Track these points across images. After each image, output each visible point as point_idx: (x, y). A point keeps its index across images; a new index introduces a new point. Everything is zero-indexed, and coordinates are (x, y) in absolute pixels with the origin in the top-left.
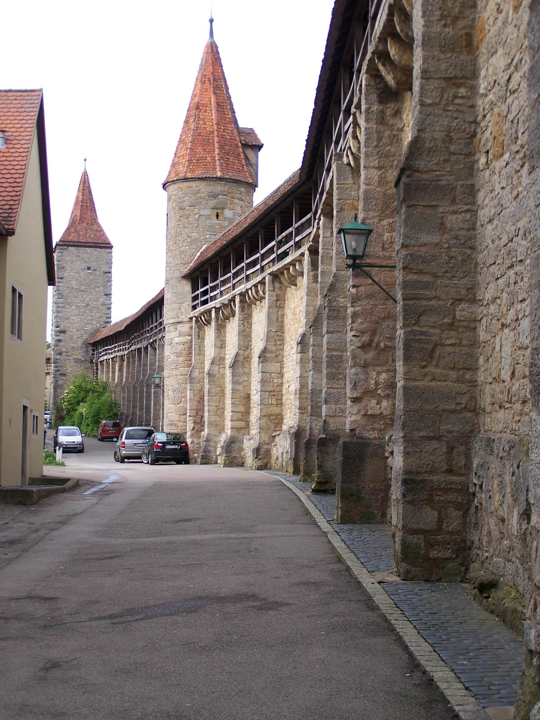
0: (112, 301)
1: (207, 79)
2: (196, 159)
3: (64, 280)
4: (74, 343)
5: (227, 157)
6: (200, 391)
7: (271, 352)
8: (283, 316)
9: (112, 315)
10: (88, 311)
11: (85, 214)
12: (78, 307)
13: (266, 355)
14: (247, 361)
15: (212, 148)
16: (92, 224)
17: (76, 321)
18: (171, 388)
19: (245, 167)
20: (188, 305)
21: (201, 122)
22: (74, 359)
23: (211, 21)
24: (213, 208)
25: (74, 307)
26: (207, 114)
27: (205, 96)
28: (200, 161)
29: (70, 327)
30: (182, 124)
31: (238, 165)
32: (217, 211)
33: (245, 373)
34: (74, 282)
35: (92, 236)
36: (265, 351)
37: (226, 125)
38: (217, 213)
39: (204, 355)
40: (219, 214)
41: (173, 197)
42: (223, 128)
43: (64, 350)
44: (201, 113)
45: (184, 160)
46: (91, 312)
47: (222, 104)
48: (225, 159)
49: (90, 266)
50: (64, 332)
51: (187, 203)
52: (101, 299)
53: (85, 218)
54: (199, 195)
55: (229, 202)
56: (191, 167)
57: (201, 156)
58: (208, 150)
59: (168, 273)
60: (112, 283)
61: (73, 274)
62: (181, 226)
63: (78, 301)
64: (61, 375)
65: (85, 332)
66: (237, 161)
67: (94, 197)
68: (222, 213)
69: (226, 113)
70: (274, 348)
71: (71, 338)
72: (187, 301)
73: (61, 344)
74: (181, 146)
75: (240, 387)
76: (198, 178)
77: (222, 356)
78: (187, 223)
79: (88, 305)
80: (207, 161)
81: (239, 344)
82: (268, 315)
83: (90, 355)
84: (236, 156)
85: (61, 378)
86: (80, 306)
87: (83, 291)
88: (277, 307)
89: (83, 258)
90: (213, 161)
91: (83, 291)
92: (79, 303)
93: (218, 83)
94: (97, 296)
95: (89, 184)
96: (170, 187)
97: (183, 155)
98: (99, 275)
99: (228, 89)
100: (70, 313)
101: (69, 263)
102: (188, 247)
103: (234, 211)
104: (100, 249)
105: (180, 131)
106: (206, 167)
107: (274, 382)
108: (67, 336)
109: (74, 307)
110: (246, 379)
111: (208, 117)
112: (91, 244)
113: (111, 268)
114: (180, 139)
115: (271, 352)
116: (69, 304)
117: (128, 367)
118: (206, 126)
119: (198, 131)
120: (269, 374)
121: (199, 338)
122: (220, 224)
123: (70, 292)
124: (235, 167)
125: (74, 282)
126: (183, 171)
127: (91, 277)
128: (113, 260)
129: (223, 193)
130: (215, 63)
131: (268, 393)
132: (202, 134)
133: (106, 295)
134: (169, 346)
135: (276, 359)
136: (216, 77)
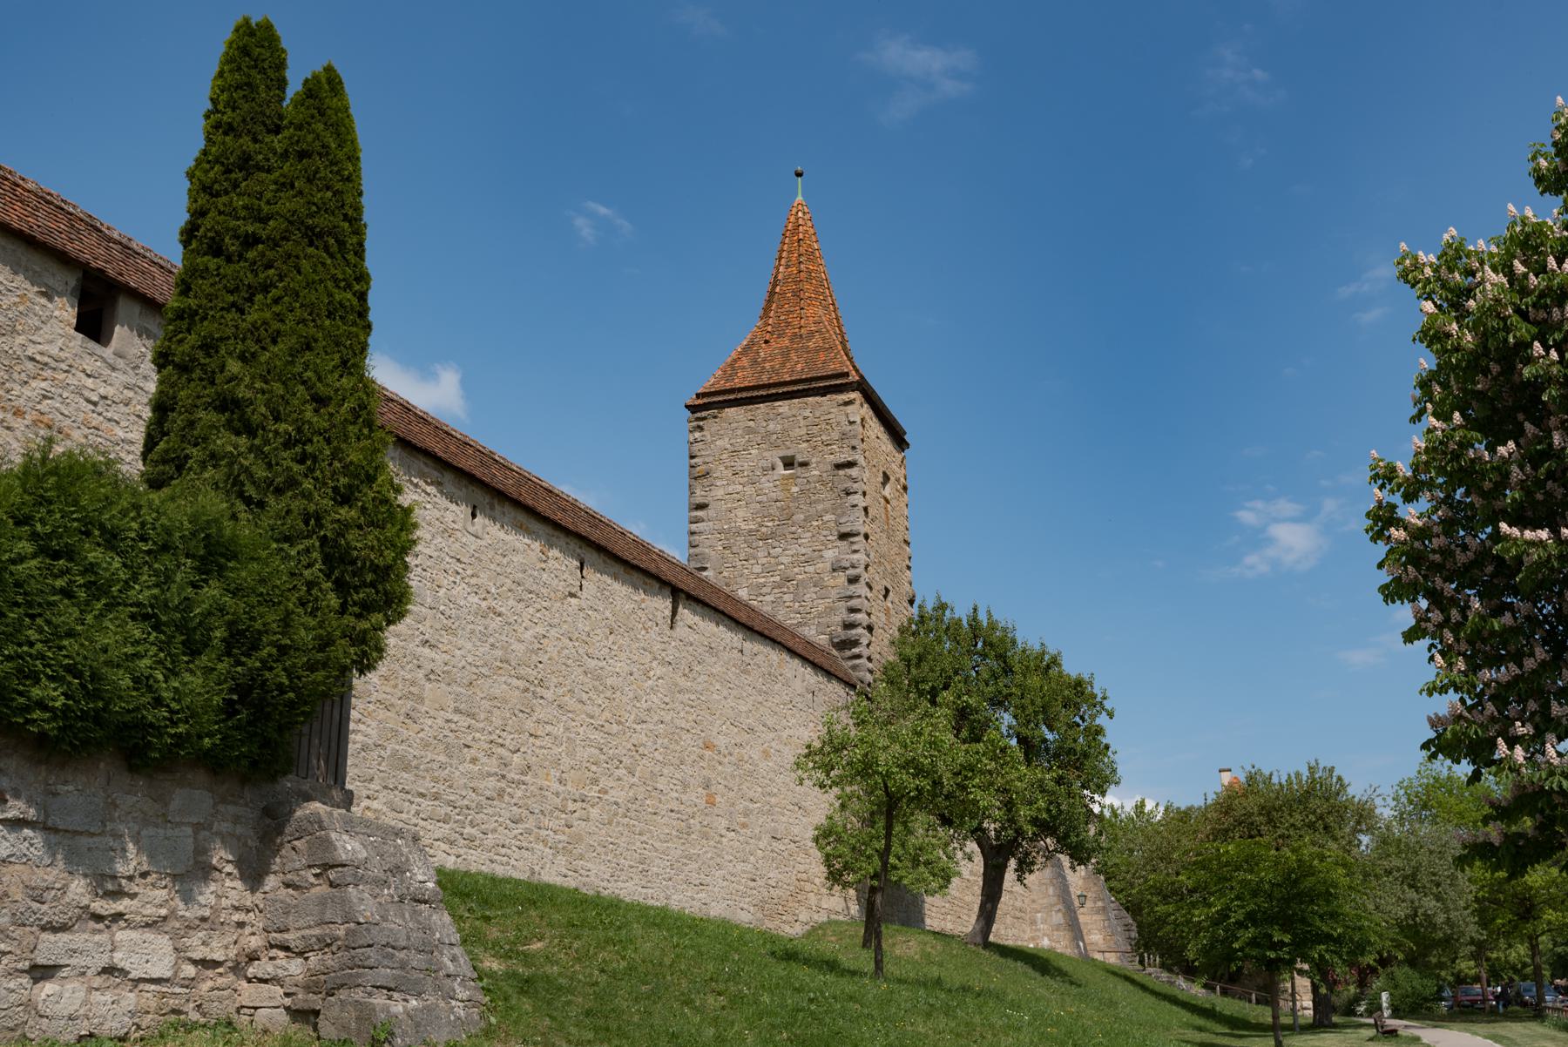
3: (710, 512)
10: (786, 597)
34: (741, 513)
49: (789, 453)
52: (830, 554)
53: (788, 324)
87: (773, 535)
91: (773, 535)
98: (820, 480)
101: (725, 456)
104: (818, 399)
127: (795, 489)
133: (843, 536)
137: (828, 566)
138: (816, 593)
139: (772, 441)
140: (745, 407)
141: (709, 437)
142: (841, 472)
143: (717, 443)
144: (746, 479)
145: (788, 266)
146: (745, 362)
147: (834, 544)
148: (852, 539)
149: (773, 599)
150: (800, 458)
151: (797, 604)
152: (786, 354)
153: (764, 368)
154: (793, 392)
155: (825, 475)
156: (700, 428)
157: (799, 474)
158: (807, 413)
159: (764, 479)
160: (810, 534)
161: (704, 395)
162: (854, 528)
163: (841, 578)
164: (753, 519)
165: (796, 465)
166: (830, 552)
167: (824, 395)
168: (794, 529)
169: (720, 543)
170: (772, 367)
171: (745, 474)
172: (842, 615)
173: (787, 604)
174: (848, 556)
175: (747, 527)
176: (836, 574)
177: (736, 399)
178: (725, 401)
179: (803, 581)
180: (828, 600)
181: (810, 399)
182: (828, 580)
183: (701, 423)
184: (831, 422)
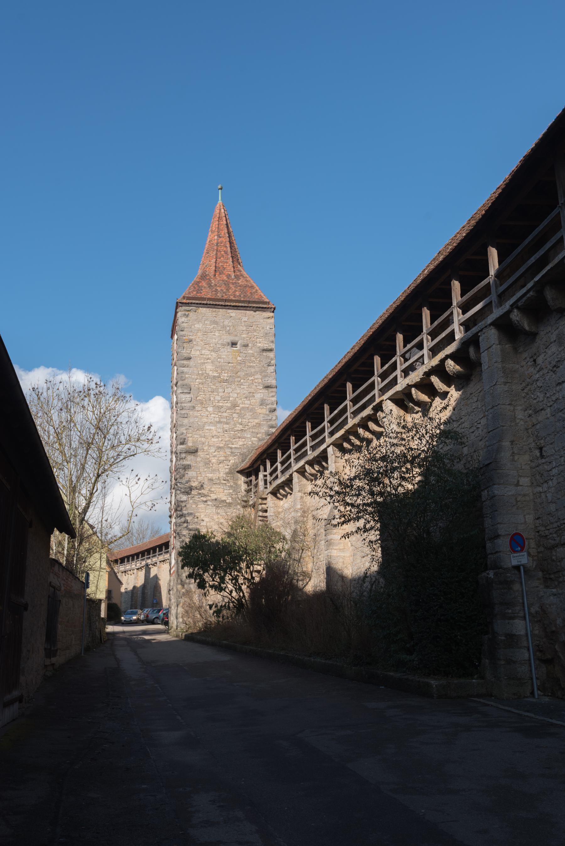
3: (191, 363)
4: (213, 471)
10: (235, 415)
25: (210, 409)
34: (209, 367)
35: (237, 293)
43: (194, 484)
50: (194, 452)
52: (258, 396)
61: (208, 352)
65: (232, 453)
71: (207, 463)
79: (234, 406)
86: (222, 407)
87: (226, 381)
89: (224, 327)
91: (226, 381)
94: (252, 390)
100: (205, 420)
101: (199, 334)
108: (199, 459)
109: (210, 409)
116: (202, 403)
125: (209, 367)
127: (240, 359)
138: (251, 415)
140: (211, 309)
142: (264, 354)
143: (196, 326)
144: (212, 348)
147: (260, 391)
148: (270, 390)
154: (239, 306)
155: (256, 354)
156: (187, 316)
157: (242, 351)
158: (245, 319)
160: (248, 383)
161: (189, 298)
163: (264, 411)
167: (255, 311)
168: (239, 379)
169: (197, 380)
170: (222, 290)
171: (212, 345)
174: (268, 398)
175: (213, 374)
176: (261, 407)
177: (206, 304)
178: (200, 304)
179: (243, 408)
180: (257, 420)
181: (248, 312)
183: (187, 313)
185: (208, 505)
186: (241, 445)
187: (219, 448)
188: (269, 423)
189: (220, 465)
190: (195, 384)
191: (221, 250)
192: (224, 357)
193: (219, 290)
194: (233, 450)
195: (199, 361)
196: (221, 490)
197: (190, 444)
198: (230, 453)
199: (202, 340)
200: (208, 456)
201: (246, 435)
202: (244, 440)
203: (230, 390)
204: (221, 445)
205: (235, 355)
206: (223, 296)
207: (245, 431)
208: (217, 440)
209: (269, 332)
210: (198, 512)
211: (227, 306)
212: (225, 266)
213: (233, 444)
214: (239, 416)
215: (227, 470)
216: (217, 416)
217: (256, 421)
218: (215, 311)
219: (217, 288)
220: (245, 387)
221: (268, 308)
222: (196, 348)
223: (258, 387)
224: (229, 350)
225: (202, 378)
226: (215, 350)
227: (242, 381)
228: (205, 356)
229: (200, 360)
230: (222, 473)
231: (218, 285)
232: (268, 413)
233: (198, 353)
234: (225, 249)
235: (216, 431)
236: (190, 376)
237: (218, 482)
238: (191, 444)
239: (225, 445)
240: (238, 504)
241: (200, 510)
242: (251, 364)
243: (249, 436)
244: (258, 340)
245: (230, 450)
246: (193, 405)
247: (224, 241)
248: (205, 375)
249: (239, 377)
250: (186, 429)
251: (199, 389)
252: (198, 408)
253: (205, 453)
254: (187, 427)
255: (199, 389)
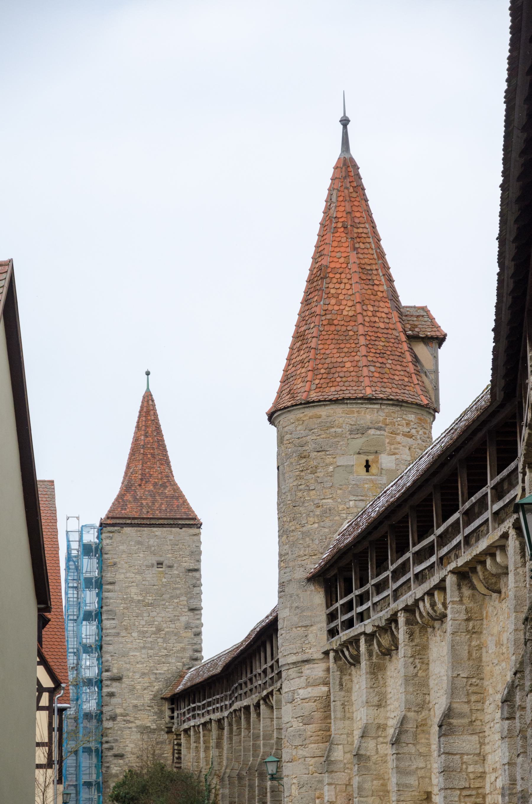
0: (204, 620)
1: (340, 225)
2: (326, 366)
3: (116, 587)
5: (380, 360)
6: (346, 785)
7: (461, 715)
8: (479, 648)
9: (203, 645)
11: (150, 468)
12: (143, 634)
13: (451, 721)
14: (423, 731)
15: (353, 345)
16: (164, 486)
17: (139, 659)
18: (295, 781)
19: (413, 375)
20: (321, 629)
21: (333, 301)
22: (137, 727)
23: (345, 122)
24: (359, 453)
25: (135, 634)
26: (342, 286)
27: (338, 255)
28: (333, 371)
29: (128, 670)
30: (298, 307)
31: (402, 373)
32: (366, 458)
33: (420, 754)
34: (134, 590)
35: (163, 507)
36: (448, 714)
37: (377, 303)
38: (367, 461)
39: (351, 719)
40: (370, 463)
41: (288, 437)
42: (371, 308)
43: (119, 711)
44: (331, 286)
45: (304, 370)
46: (165, 641)
47: (368, 267)
48: (378, 365)
49: (161, 559)
50: (118, 679)
51: (311, 446)
52: (183, 619)
53: (151, 476)
54: (333, 430)
55: (387, 441)
56: (317, 381)
57: (334, 360)
58: (346, 350)
59: (282, 572)
60: (202, 588)
62: (303, 486)
63: (143, 623)
64: (116, 756)
65: (156, 678)
66: (399, 368)
67: (165, 438)
68: (376, 461)
69: (376, 282)
70: (466, 708)
71: (132, 689)
72: (318, 623)
73: (114, 701)
74: (298, 344)
75: (412, 781)
76: (330, 400)
77: (382, 721)
78: (313, 481)
80: (344, 369)
81: (407, 701)
82: (453, 646)
83: (167, 719)
84: (396, 358)
85: (115, 761)
86: (147, 632)
87: (151, 605)
88: (468, 631)
89: (149, 547)
90: (356, 369)
91: (151, 605)
92: (143, 627)
93: (360, 230)
94: (176, 613)
95: (156, 415)
96: (281, 418)
97: (302, 362)
98: (178, 576)
99: (379, 240)
100: (129, 646)
101: (124, 556)
102: (316, 525)
103: (397, 456)
105: (295, 318)
106: (344, 379)
107: (469, 770)
108: (124, 686)
109: (135, 634)
110: (422, 765)
111: (344, 292)
112: (161, 522)
113: (199, 561)
114: (297, 332)
115: (461, 715)
116: (126, 629)
117: (231, 739)
118: (342, 307)
119: (328, 317)
120: (458, 757)
121: (341, 689)
122: (372, 481)
123: (127, 608)
124: (396, 378)
126: (303, 390)
128: (202, 548)
129: (377, 425)
130: (354, 195)
131: (458, 792)
132: (336, 322)
133: (192, 610)
134: (289, 705)
135: (471, 727)
136: (357, 221)
137: (183, 624)
139: (152, 551)
140: (136, 528)
141: (115, 543)
142: (190, 574)
143: (120, 547)
144: (137, 571)
145: (146, 436)
146: (129, 497)
147: (186, 614)
149: (151, 640)
150: (166, 562)
151: (165, 645)
152: (153, 496)
153: (142, 503)
155: (181, 574)
156: (111, 538)
157: (167, 572)
158: (171, 537)
159: (147, 572)
161: (113, 518)
162: (197, 606)
163: (190, 634)
164: (141, 594)
165: (164, 566)
166: (184, 617)
167: (181, 528)
168: (164, 602)
169: (122, 605)
171: (136, 568)
172: (189, 653)
173: (160, 644)
175: (137, 598)
176: (186, 630)
178: (125, 524)
179: (168, 632)
181: (173, 529)
182: (183, 633)
183: (111, 535)
184: (185, 544)
185: (132, 731)
186: (165, 671)
187: (144, 674)
188: (194, 647)
189: (145, 691)
190: (120, 609)
191: (148, 453)
192: (149, 579)
193: (144, 504)
194: (158, 676)
195: (124, 585)
196: (146, 716)
197: (115, 671)
198: (154, 679)
199: (126, 563)
200: (133, 683)
201: (170, 660)
202: (168, 664)
203: (154, 614)
204: (146, 671)
205: (160, 577)
206: (148, 512)
207: (170, 655)
208: (142, 666)
209: (195, 550)
210: (123, 739)
211: (153, 524)
212: (152, 473)
213: (157, 670)
214: (164, 641)
215: (151, 696)
216: (142, 641)
217: (182, 645)
218: (139, 531)
219: (143, 502)
220: (170, 610)
221: (195, 524)
222: (121, 571)
223: (183, 610)
224: (154, 572)
225: (127, 602)
226: (139, 573)
227: (167, 604)
228: (129, 580)
229: (125, 584)
230: (146, 699)
231: (143, 497)
232: (193, 636)
233: (122, 576)
234: (152, 451)
235: (141, 656)
236: (115, 601)
237: (143, 708)
238: (116, 671)
239: (149, 671)
240: (163, 730)
241: (125, 737)
242: (177, 586)
243: (173, 661)
244: (184, 559)
245: (155, 676)
246: (117, 631)
247: (152, 441)
248: (130, 599)
249: (163, 600)
250: (111, 656)
251: (123, 614)
252: (123, 633)
253: (130, 680)
254: (112, 654)
255: (123, 614)
